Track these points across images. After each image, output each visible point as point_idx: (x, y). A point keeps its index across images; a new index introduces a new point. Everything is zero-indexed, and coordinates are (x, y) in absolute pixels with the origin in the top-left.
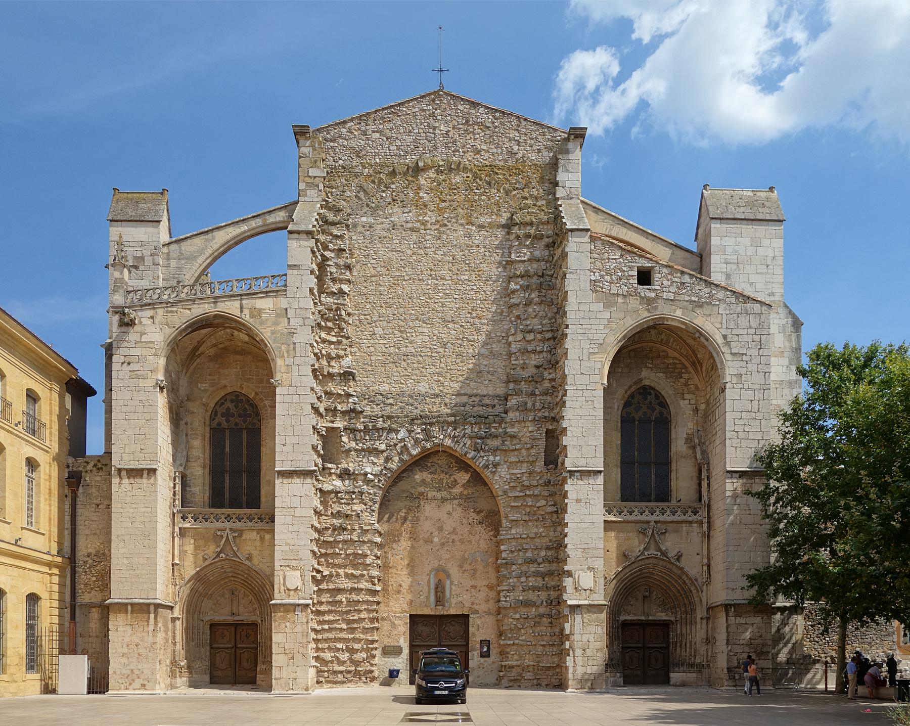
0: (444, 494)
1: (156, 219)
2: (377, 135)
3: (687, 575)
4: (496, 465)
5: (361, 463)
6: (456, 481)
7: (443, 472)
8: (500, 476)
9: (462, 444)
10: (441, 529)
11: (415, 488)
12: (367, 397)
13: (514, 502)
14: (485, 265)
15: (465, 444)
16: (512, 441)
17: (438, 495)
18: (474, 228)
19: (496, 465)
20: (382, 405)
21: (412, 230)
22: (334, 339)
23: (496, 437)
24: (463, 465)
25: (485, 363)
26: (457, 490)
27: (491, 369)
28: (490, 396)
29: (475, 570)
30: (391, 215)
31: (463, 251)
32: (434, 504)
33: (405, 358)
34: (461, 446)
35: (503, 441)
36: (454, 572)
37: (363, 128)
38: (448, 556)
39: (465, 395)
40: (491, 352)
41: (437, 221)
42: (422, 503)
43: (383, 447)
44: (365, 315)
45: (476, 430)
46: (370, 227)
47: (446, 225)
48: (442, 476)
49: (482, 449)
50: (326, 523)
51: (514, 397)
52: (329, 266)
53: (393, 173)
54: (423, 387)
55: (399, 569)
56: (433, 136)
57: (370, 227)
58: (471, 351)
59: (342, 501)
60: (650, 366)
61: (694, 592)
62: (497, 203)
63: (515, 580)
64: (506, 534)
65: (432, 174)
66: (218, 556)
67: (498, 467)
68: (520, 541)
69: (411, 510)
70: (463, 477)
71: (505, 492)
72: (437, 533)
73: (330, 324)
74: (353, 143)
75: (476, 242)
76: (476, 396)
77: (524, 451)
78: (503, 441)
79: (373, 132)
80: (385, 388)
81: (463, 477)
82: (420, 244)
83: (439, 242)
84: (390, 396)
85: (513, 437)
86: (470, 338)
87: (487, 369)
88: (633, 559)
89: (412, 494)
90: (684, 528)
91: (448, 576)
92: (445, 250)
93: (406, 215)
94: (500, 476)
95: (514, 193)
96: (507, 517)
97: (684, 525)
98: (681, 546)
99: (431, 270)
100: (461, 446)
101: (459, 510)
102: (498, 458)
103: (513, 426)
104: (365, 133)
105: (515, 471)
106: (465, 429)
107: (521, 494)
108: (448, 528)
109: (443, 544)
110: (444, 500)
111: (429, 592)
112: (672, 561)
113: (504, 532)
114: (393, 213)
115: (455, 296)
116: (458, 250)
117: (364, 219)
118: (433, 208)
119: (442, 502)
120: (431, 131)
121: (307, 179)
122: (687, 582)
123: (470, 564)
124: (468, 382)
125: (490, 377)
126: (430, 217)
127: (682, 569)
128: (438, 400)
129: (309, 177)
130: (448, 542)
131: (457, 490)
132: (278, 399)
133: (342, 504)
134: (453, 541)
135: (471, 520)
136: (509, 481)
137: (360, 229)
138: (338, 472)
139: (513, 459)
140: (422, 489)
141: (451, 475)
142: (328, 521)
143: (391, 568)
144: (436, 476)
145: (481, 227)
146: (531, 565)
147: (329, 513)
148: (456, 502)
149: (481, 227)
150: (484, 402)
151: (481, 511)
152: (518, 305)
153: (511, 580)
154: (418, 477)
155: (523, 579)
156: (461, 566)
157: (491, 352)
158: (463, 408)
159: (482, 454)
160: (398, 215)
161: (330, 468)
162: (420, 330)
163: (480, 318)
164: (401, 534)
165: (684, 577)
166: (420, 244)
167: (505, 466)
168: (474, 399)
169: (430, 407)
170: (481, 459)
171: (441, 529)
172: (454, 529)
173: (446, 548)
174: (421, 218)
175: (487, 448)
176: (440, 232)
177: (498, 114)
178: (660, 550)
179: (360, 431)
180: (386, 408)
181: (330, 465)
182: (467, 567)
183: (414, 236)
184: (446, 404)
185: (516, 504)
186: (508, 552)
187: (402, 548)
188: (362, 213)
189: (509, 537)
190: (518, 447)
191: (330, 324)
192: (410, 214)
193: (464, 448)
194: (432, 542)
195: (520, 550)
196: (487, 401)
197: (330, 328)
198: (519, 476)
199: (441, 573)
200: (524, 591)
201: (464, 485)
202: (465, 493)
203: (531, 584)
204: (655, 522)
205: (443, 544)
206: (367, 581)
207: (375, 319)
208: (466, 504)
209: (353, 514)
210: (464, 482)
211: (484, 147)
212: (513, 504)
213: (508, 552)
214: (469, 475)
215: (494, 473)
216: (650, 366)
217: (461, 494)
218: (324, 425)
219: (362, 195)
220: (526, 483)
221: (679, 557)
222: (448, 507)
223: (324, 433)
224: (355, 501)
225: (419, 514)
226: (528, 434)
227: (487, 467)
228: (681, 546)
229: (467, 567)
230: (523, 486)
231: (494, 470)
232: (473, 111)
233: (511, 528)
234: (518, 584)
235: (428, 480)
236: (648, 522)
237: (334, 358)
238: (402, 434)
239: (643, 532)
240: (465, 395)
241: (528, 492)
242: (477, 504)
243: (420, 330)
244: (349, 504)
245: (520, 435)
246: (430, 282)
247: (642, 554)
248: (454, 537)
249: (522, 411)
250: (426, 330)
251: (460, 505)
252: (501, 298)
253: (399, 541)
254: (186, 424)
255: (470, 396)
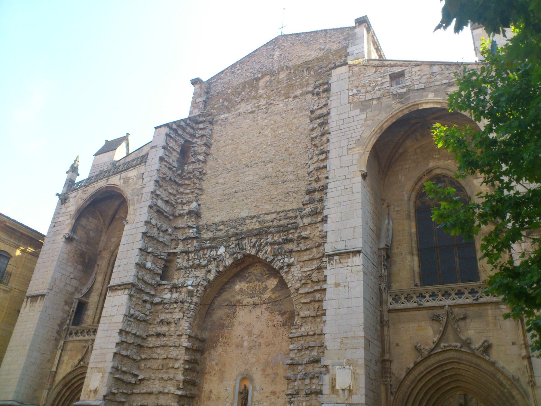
0: (256, 300)
1: (115, 148)
2: (240, 71)
3: (503, 374)
4: (289, 265)
5: (187, 278)
6: (266, 287)
7: (257, 280)
8: (293, 276)
9: (264, 251)
10: (250, 333)
11: (233, 296)
12: (206, 227)
13: (305, 298)
14: (296, 120)
15: (267, 251)
16: (305, 242)
17: (251, 301)
18: (290, 99)
19: (289, 265)
20: (214, 231)
21: (250, 113)
22: (188, 191)
23: (291, 241)
24: (275, 273)
25: (292, 185)
26: (266, 296)
27: (296, 189)
28: (293, 209)
29: (276, 374)
30: (239, 109)
31: (281, 115)
32: (247, 309)
33: (235, 194)
34: (263, 253)
35: (298, 244)
36: (258, 377)
37: (232, 71)
38: (254, 360)
39: (274, 213)
40: (297, 177)
41: (267, 103)
42: (238, 309)
43: (204, 263)
44: (214, 172)
45: (276, 238)
46: (226, 119)
47: (271, 104)
48: (256, 283)
49: (279, 253)
50: (152, 331)
51: (309, 206)
52: (193, 147)
53: (244, 87)
54: (244, 214)
55: (213, 374)
56: (272, 60)
57: (226, 119)
58: (282, 179)
59: (167, 311)
60: (437, 156)
61: (518, 397)
62: (307, 80)
63: (300, 382)
64: (296, 332)
65: (267, 78)
66: (79, 363)
67: (292, 267)
68: (308, 338)
69: (228, 317)
70: (272, 283)
71: (297, 290)
72: (246, 338)
73: (187, 182)
74: (225, 80)
75: (291, 107)
76: (283, 211)
77: (315, 250)
78: (298, 244)
79: (238, 70)
80: (217, 220)
81: (272, 283)
82: (254, 120)
83: (266, 115)
84: (221, 223)
85: (306, 238)
86: (282, 170)
87: (293, 189)
88: (426, 353)
89: (231, 302)
90: (490, 312)
91: (252, 381)
92: (269, 118)
93: (248, 106)
94: (293, 276)
95: (320, 71)
96: (298, 315)
97: (489, 307)
98: (489, 334)
99: (260, 133)
100: (263, 253)
101: (266, 314)
102: (292, 260)
103: (306, 230)
104: (233, 72)
105: (306, 269)
106: (267, 239)
107: (310, 290)
108: (256, 331)
109: (250, 348)
110: (255, 305)
111: (234, 396)
112: (478, 353)
113: (294, 331)
114: (240, 107)
115: (274, 145)
116: (279, 116)
117: (222, 116)
118: (265, 96)
119: (254, 308)
120: (271, 57)
121: (195, 105)
122: (505, 382)
123: (272, 369)
124: (277, 202)
125: (295, 195)
126: (263, 102)
127: (493, 364)
128: (255, 220)
129: (196, 103)
130: (254, 346)
131: (266, 296)
132: (125, 233)
133: (166, 313)
134: (260, 345)
135: (275, 322)
136: (300, 279)
137: (219, 122)
138: (169, 287)
139: (306, 258)
140: (239, 297)
141: (263, 282)
142: (154, 329)
143: (207, 373)
144: (251, 285)
145: (295, 97)
146: (316, 365)
147: (156, 322)
148: (265, 306)
149: (295, 97)
150: (288, 215)
151: (285, 313)
152: (316, 137)
153: (296, 383)
154: (238, 286)
155: (307, 381)
156: (264, 370)
157: (297, 177)
158: (271, 223)
159: (279, 257)
160: (243, 107)
161: (164, 285)
162: (247, 173)
163: (290, 155)
164: (218, 340)
165: (499, 375)
166: (254, 120)
167: (298, 266)
168: (281, 214)
169: (248, 227)
170: (278, 262)
171: (250, 333)
172: (262, 332)
173: (253, 352)
174: (256, 105)
175: (283, 251)
176: (267, 109)
177: (313, 34)
178: (459, 340)
179: (191, 252)
180: (217, 234)
181: (164, 282)
182: (269, 371)
183: (251, 116)
184: (259, 222)
185: (305, 301)
186: (296, 351)
187: (218, 353)
188: (222, 113)
189: (296, 335)
190: (308, 247)
191: (187, 182)
192: (251, 105)
193: (267, 253)
194: (242, 346)
195: (307, 348)
196: (291, 214)
197: (188, 185)
198: (309, 273)
199: (246, 377)
200: (307, 395)
201: (272, 290)
202: (273, 296)
203: (314, 387)
204: (451, 306)
205: (250, 348)
206: (174, 386)
207: (220, 173)
208: (273, 308)
209: (173, 321)
210: (273, 287)
211: (304, 54)
212: (303, 301)
213: (296, 351)
214: (277, 280)
215: (287, 272)
216: (437, 156)
217: (270, 298)
218: (166, 251)
219: (226, 104)
220: (315, 279)
221: (487, 348)
222: (258, 311)
223: (162, 257)
224: (176, 311)
225: (234, 320)
226: (318, 234)
227: (281, 268)
228: (489, 334)
229: (269, 371)
230: (312, 281)
231: (287, 270)
232: (297, 39)
233: (301, 325)
234: (302, 388)
235: (245, 288)
236: (442, 307)
237: (186, 203)
238: (222, 250)
239: (436, 319)
240: (274, 213)
241: (316, 288)
242: (282, 307)
243: (247, 173)
244: (171, 313)
245: (312, 236)
246: (258, 140)
247: (437, 344)
248: (261, 340)
249: (313, 215)
250: (251, 173)
251: (268, 308)
252: (307, 137)
253: (216, 346)
254: (98, 265)
255: (278, 213)
